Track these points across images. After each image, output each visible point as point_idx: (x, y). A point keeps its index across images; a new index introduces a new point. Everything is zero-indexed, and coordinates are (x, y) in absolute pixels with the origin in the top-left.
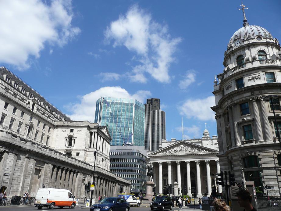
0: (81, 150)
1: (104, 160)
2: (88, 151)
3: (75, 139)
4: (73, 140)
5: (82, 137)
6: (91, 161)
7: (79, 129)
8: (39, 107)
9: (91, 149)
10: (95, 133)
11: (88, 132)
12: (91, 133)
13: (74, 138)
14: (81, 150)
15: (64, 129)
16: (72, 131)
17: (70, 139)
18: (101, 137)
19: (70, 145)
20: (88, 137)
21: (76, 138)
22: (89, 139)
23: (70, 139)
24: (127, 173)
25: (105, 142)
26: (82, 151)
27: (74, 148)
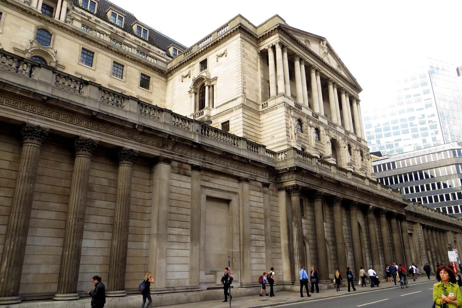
0: (231, 111)
1: (343, 144)
2: (263, 112)
3: (213, 86)
4: (207, 88)
5: (230, 70)
6: (275, 141)
7: (220, 50)
8: (91, 18)
9: (271, 103)
10: (274, 48)
11: (253, 53)
12: (264, 55)
13: (208, 80)
14: (231, 111)
15: (184, 71)
16: (204, 64)
17: (202, 90)
18: (308, 69)
19: (202, 105)
20: (257, 70)
21: (216, 79)
22: (259, 74)
23: (202, 90)
24: (447, 204)
25: (333, 93)
26: (235, 113)
27: (213, 112)
